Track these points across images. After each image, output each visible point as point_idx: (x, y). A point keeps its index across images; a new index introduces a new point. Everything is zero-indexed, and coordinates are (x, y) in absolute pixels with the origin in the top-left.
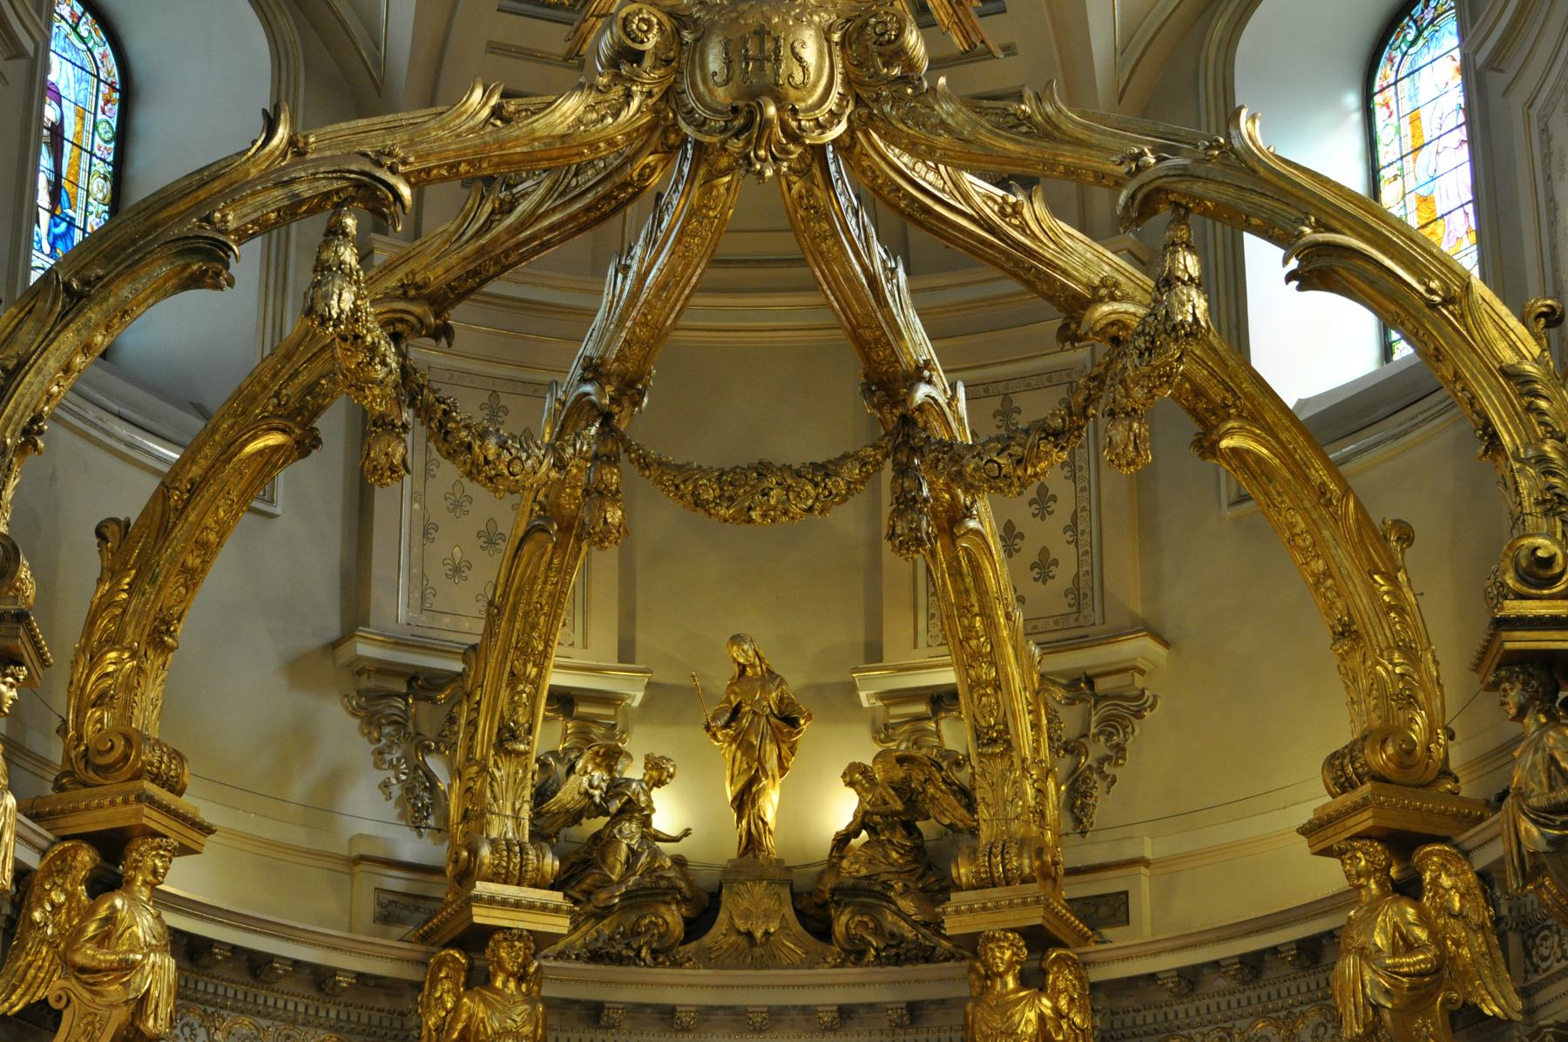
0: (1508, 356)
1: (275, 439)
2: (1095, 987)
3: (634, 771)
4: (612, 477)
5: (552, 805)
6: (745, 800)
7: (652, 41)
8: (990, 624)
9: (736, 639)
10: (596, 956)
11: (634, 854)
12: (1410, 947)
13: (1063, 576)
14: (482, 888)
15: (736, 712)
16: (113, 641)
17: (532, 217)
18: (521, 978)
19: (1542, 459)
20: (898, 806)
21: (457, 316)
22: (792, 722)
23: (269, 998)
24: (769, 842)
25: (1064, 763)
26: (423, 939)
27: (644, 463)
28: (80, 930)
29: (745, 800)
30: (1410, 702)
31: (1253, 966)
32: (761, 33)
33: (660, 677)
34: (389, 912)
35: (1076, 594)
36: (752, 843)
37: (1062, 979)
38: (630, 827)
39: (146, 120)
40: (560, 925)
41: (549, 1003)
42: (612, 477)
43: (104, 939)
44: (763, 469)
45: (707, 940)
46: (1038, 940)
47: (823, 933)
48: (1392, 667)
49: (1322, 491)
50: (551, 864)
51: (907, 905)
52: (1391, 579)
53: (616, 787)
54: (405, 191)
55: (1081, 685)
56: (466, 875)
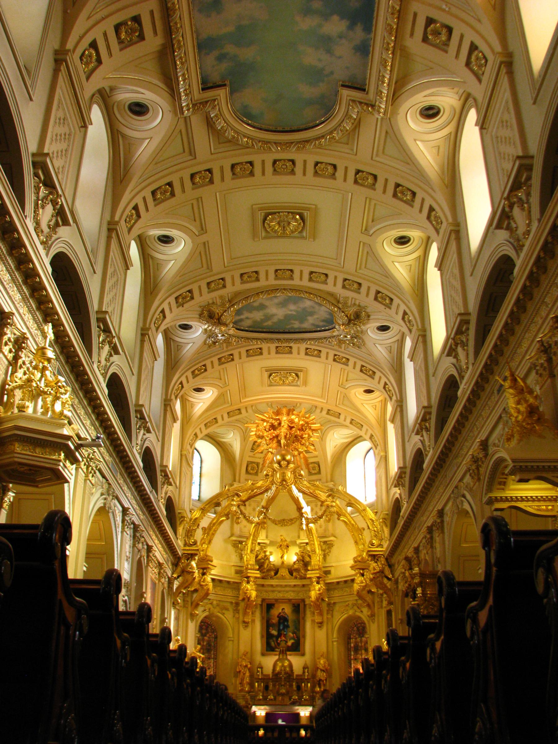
0: (371, 517)
1: (224, 518)
2: (326, 583)
3: (268, 553)
4: (265, 520)
5: (258, 559)
6: (282, 557)
7: (270, 474)
8: (313, 537)
9: (281, 536)
10: (263, 578)
11: (268, 565)
12: (362, 583)
13: (323, 528)
14: (249, 571)
15: (281, 546)
16: (204, 543)
17: (256, 492)
18: (254, 582)
19: (374, 530)
20: (301, 558)
21: (247, 503)
22: (288, 547)
23: (221, 584)
24: (285, 563)
25: (323, 553)
26: (241, 576)
27: (269, 519)
28: (200, 580)
29: (282, 557)
30: (363, 551)
31: (346, 582)
32: (284, 473)
33: (272, 540)
34: (237, 572)
35: (325, 531)
36: (283, 563)
37: (321, 582)
38: (267, 561)
39: (203, 465)
40: (259, 575)
41: (257, 584)
42: (265, 520)
43: (203, 582)
44: (284, 520)
45: (277, 576)
46: (319, 578)
47: (291, 574)
48: (361, 547)
49: (353, 525)
50: (257, 567)
51: (303, 571)
52: (361, 535)
53: (266, 556)
54: (241, 494)
55: (325, 542)
56: (247, 569)
